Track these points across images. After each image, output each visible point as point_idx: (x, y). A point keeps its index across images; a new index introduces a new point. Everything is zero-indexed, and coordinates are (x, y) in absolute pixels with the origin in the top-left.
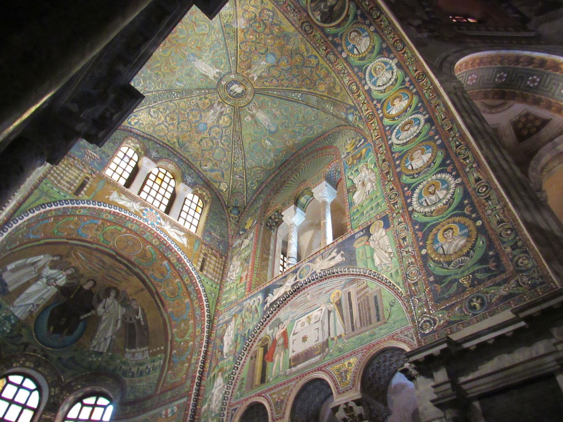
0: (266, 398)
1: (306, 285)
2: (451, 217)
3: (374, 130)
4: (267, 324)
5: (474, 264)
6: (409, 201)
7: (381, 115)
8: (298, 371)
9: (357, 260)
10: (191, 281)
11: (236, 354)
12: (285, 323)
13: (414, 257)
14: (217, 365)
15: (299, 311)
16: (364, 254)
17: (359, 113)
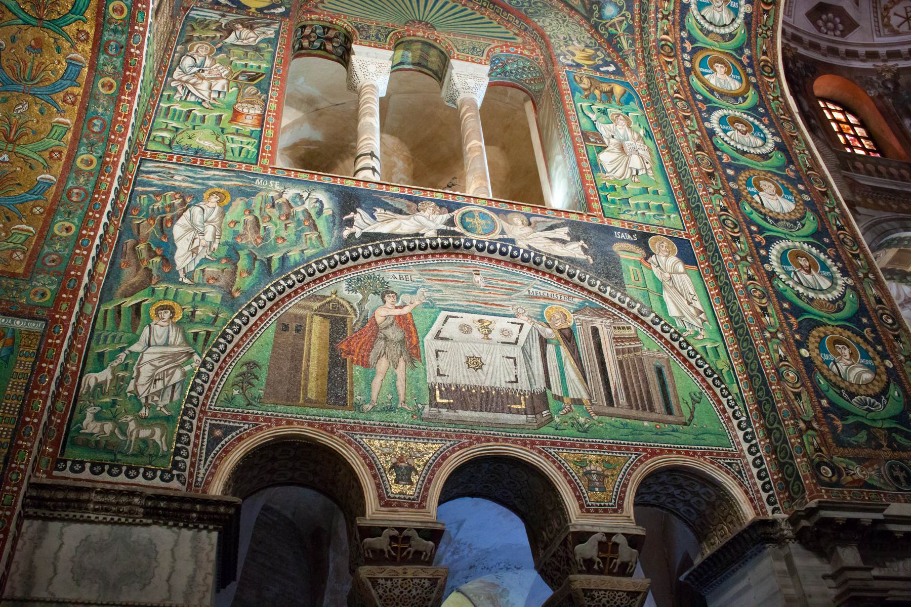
0: (350, 443)
1: (477, 253)
2: (844, 327)
3: (671, 78)
4: (341, 271)
5: (890, 418)
6: (763, 252)
7: (688, 65)
8: (460, 422)
9: (626, 281)
10: (132, 20)
11: (237, 295)
12: (405, 298)
13: (788, 349)
14: (146, 283)
15: (454, 297)
16: (641, 279)
17: (633, 19)
